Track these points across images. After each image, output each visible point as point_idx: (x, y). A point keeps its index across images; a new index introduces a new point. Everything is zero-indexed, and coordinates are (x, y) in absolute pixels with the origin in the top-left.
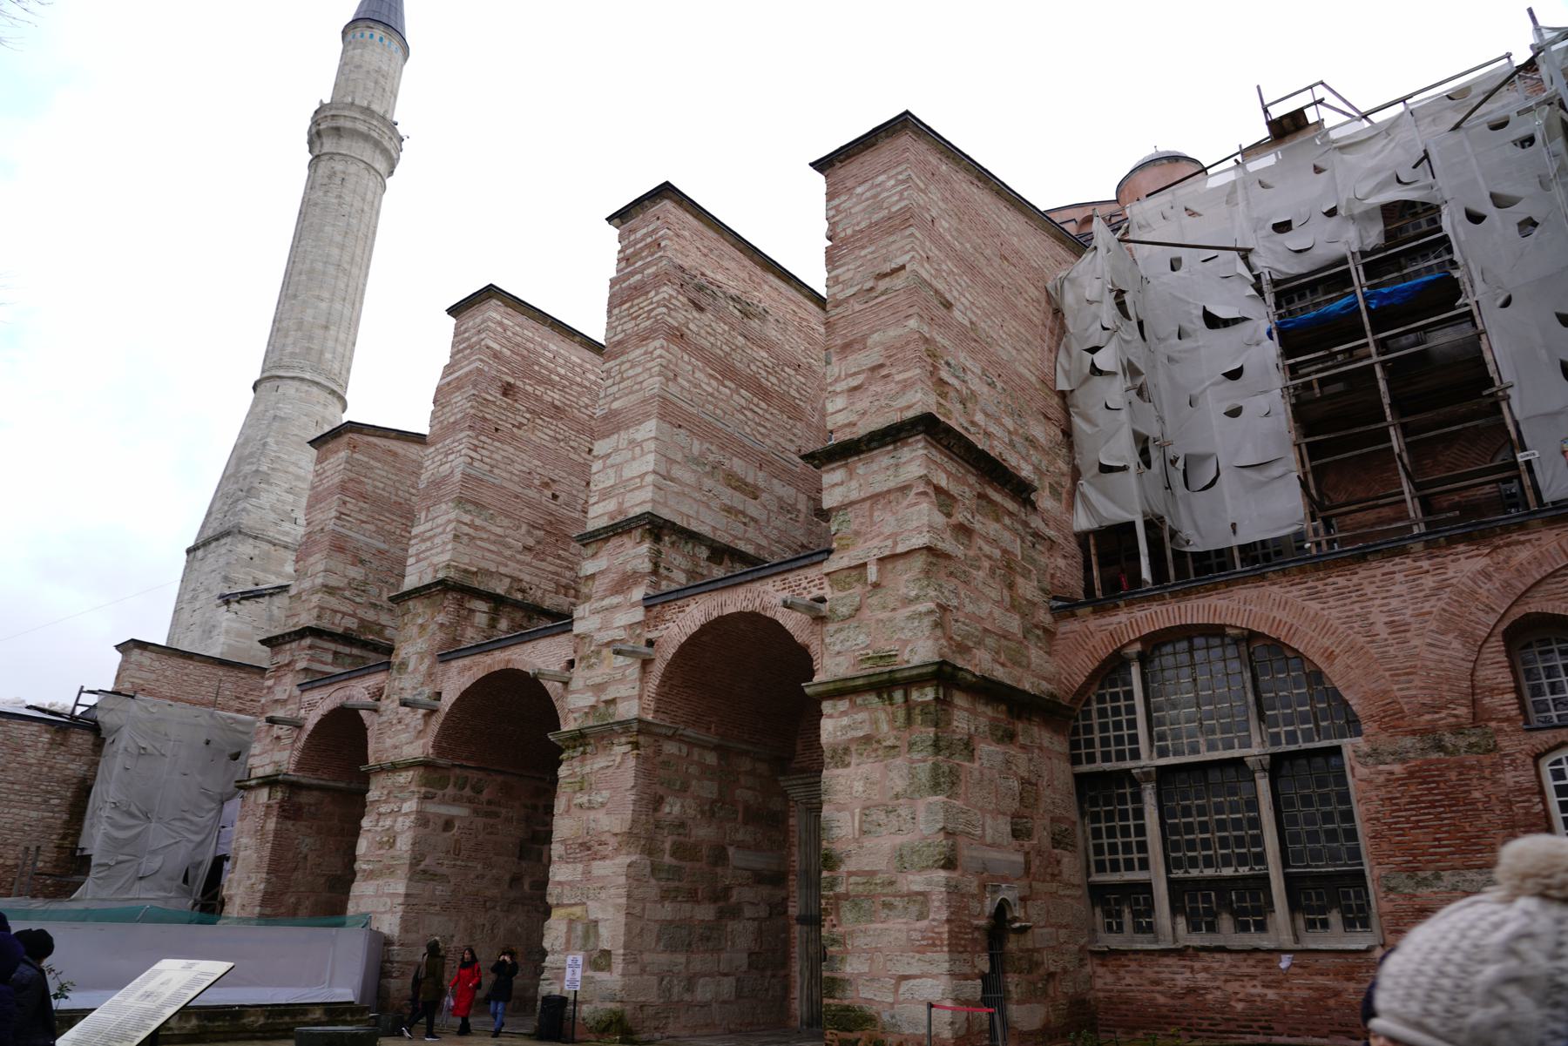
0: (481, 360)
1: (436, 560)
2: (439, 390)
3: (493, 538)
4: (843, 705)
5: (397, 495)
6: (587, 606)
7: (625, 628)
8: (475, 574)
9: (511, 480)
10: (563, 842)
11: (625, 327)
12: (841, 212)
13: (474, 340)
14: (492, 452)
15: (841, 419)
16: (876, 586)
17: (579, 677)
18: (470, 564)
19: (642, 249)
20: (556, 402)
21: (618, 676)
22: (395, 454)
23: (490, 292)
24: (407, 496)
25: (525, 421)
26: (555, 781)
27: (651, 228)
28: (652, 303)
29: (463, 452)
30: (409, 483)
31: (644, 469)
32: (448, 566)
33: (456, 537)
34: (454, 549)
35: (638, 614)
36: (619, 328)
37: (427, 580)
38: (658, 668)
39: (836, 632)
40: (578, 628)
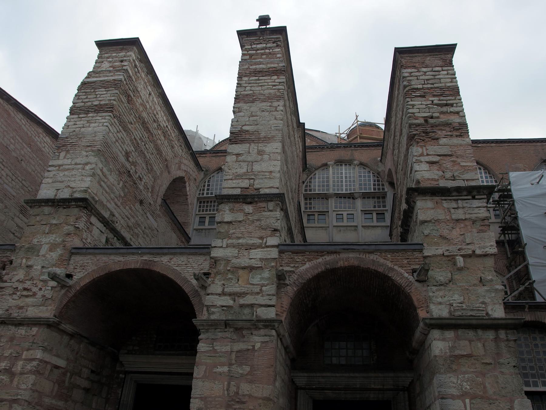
0: (124, 77)
1: (73, 185)
2: (84, 84)
3: (108, 183)
4: (449, 334)
5: (3, 139)
6: (225, 241)
7: (261, 260)
8: (96, 202)
9: (121, 153)
10: (201, 398)
11: (253, 89)
12: (412, 76)
13: (117, 64)
14: (117, 131)
15: (427, 175)
16: (460, 269)
17: (216, 286)
18: (96, 195)
19: (262, 54)
20: (146, 119)
21: (258, 290)
22: (9, 114)
23: (135, 43)
24: (9, 143)
25: (133, 122)
26: (194, 352)
27: (269, 45)
28: (274, 82)
29: (105, 124)
30: (12, 135)
31: (272, 169)
32: (86, 191)
33: (93, 175)
34: (91, 181)
35: (274, 254)
36: (248, 88)
37: (65, 194)
38: (291, 290)
39: (436, 290)
40: (215, 253)
